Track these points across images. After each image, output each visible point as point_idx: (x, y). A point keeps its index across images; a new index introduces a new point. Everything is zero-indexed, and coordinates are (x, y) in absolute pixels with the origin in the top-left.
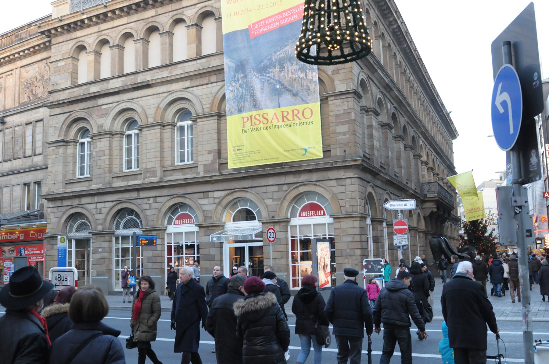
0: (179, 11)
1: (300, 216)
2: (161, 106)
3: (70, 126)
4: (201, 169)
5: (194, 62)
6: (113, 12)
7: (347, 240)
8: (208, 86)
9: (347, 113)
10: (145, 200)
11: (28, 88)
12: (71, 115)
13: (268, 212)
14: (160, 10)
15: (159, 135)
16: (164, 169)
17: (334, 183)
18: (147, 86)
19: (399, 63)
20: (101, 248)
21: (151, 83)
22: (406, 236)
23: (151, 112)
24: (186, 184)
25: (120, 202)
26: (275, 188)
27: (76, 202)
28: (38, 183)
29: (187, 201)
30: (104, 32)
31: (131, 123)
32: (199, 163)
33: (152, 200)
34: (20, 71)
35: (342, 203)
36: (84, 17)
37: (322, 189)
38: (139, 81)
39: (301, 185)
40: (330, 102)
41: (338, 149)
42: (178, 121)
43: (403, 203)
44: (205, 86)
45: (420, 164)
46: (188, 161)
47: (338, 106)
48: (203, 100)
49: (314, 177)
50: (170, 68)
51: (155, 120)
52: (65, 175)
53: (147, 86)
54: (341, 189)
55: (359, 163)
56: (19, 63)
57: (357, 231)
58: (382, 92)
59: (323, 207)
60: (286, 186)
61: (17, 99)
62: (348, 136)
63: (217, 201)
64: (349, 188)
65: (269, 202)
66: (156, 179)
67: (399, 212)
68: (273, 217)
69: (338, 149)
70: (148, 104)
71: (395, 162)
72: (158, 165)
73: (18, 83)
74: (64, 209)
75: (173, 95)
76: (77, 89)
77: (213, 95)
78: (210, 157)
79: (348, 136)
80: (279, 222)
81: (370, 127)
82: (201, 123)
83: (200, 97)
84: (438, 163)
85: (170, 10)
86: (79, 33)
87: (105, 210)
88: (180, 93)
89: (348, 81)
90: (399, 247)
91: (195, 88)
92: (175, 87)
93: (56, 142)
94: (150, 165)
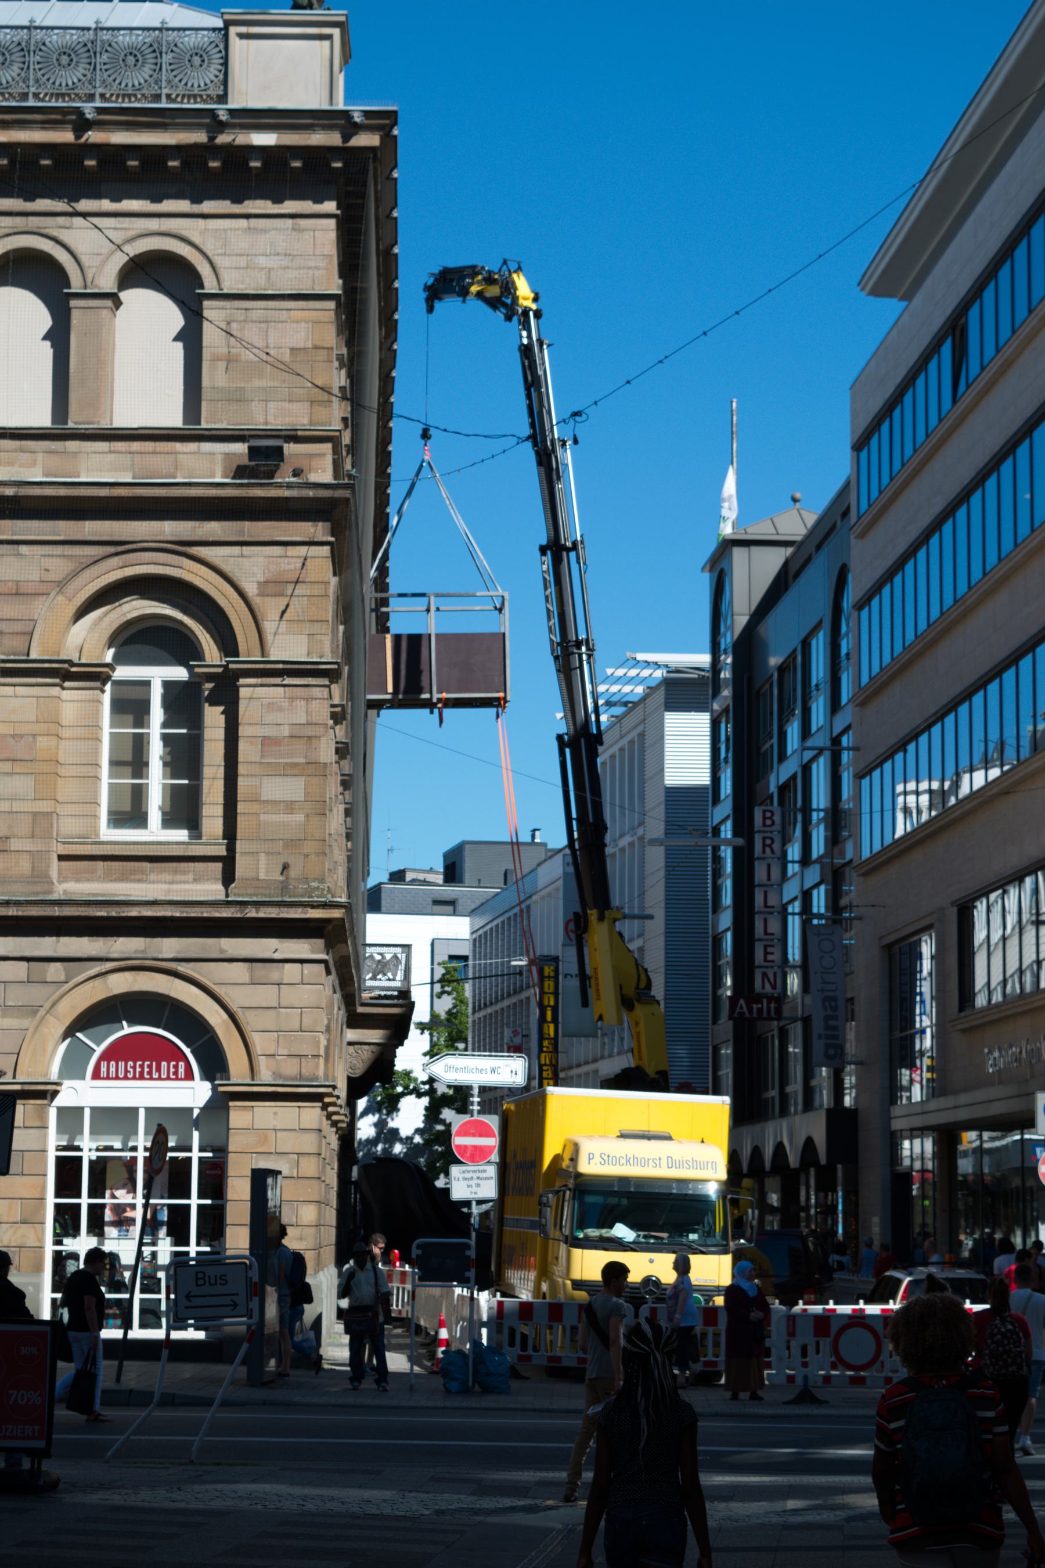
1: (96, 1075)
9: (303, 737)
17: (240, 970)
40: (243, 692)
47: (271, 707)
49: (169, 947)
54: (266, 995)
59: (187, 1051)
60: (58, 964)
64: (290, 996)
67: (476, 1091)
69: (263, 857)
79: (299, 818)
89: (316, 628)
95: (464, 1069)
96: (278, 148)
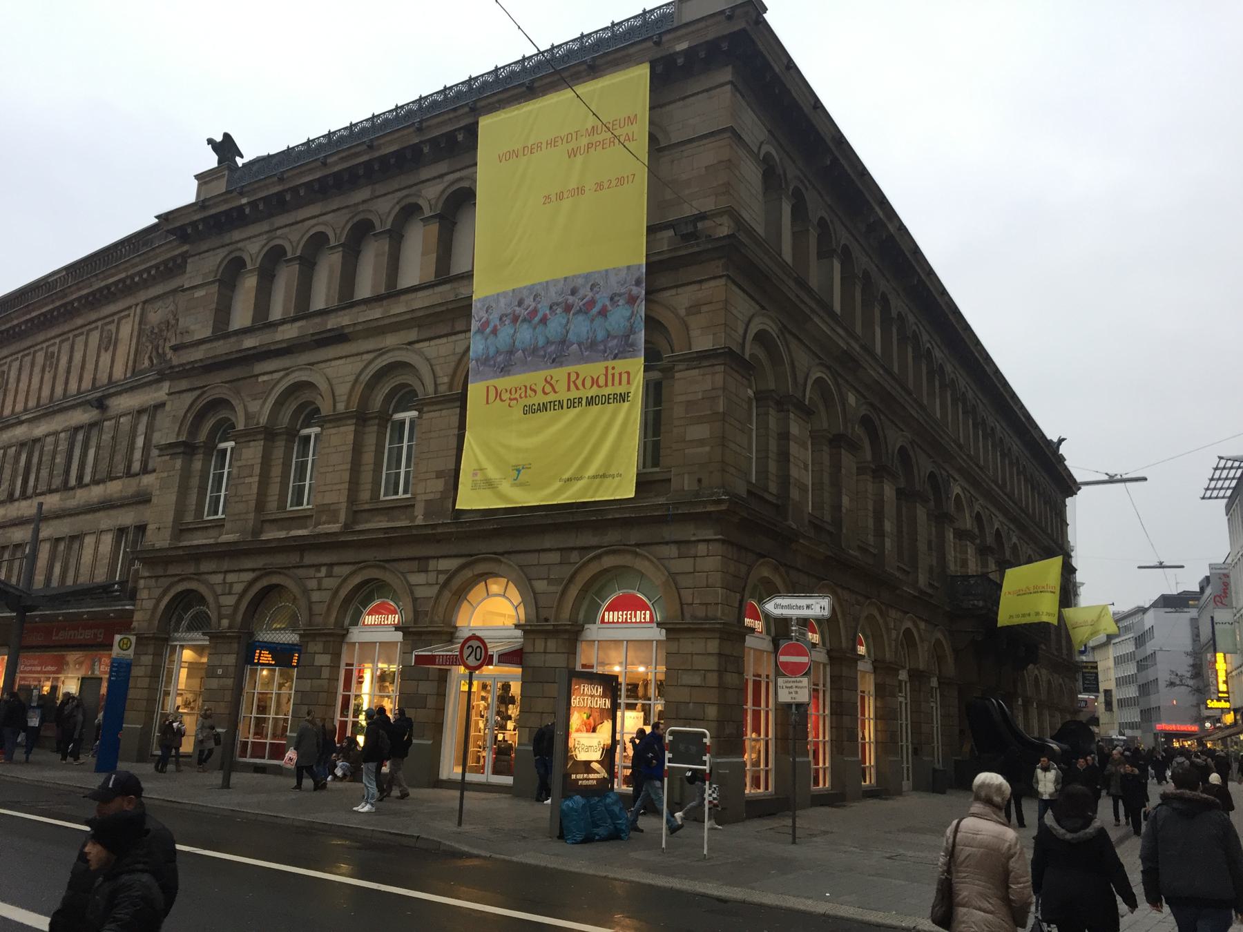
0: (414, 188)
2: (362, 378)
3: (200, 417)
4: (419, 512)
5: (429, 292)
6: (295, 190)
7: (690, 683)
8: (454, 338)
10: (312, 572)
12: (204, 393)
13: (537, 608)
14: (381, 189)
15: (352, 437)
16: (355, 508)
17: (673, 551)
18: (339, 337)
19: (894, 314)
20: (220, 666)
21: (346, 331)
22: (805, 681)
23: (342, 390)
24: (390, 539)
25: (266, 572)
26: (554, 557)
27: (190, 569)
28: (141, 529)
29: (387, 577)
30: (279, 232)
31: (311, 414)
32: (419, 498)
33: (324, 570)
34: (143, 309)
35: (687, 595)
36: (244, 201)
37: (647, 563)
38: (329, 327)
39: (607, 553)
40: (677, 375)
41: (686, 476)
42: (396, 411)
43: (803, 602)
44: (444, 340)
45: (950, 535)
46: (405, 492)
48: (437, 369)
49: (635, 536)
50: (385, 303)
51: (347, 408)
52: (180, 511)
53: (339, 337)
54: (686, 565)
55: (723, 507)
56: (143, 295)
57: (712, 663)
58: (828, 368)
61: (131, 363)
62: (707, 449)
63: (442, 578)
65: (541, 586)
66: (335, 527)
68: (546, 620)
69: (686, 476)
70: (339, 375)
71: (871, 522)
72: (343, 499)
73: (135, 333)
74: (165, 582)
75: (385, 357)
76: (221, 342)
77: (456, 358)
78: (439, 485)
79: (707, 449)
80: (556, 632)
81: (784, 436)
82: (431, 415)
83: (433, 362)
84: (1014, 540)
85: (397, 187)
86: (236, 235)
87: (238, 588)
88: (397, 353)
90: (789, 705)
91: (427, 344)
92: (390, 340)
93: (171, 445)
94: (329, 499)
95: (789, 607)
96: (690, 48)
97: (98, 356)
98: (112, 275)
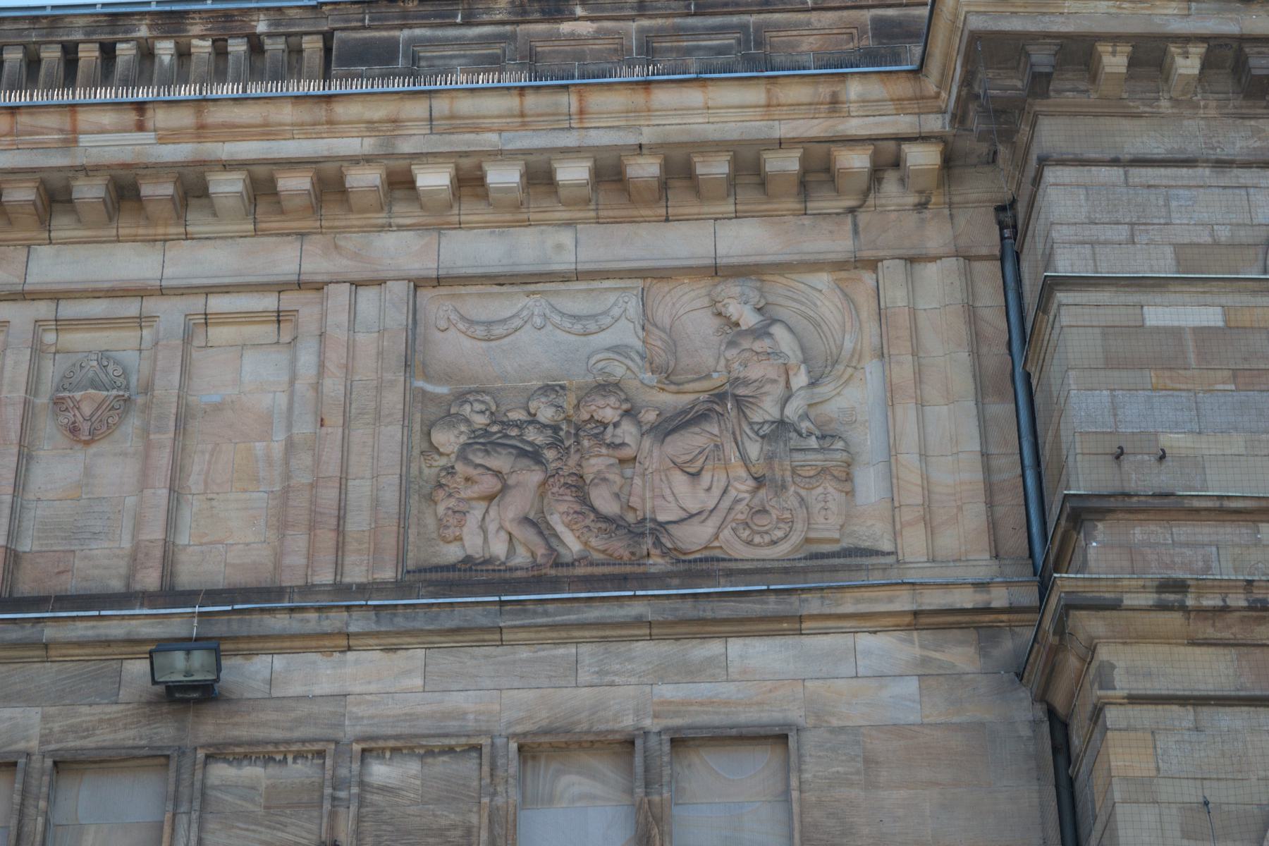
11: (535, 456)
97: (25, 457)
98: (267, 131)
